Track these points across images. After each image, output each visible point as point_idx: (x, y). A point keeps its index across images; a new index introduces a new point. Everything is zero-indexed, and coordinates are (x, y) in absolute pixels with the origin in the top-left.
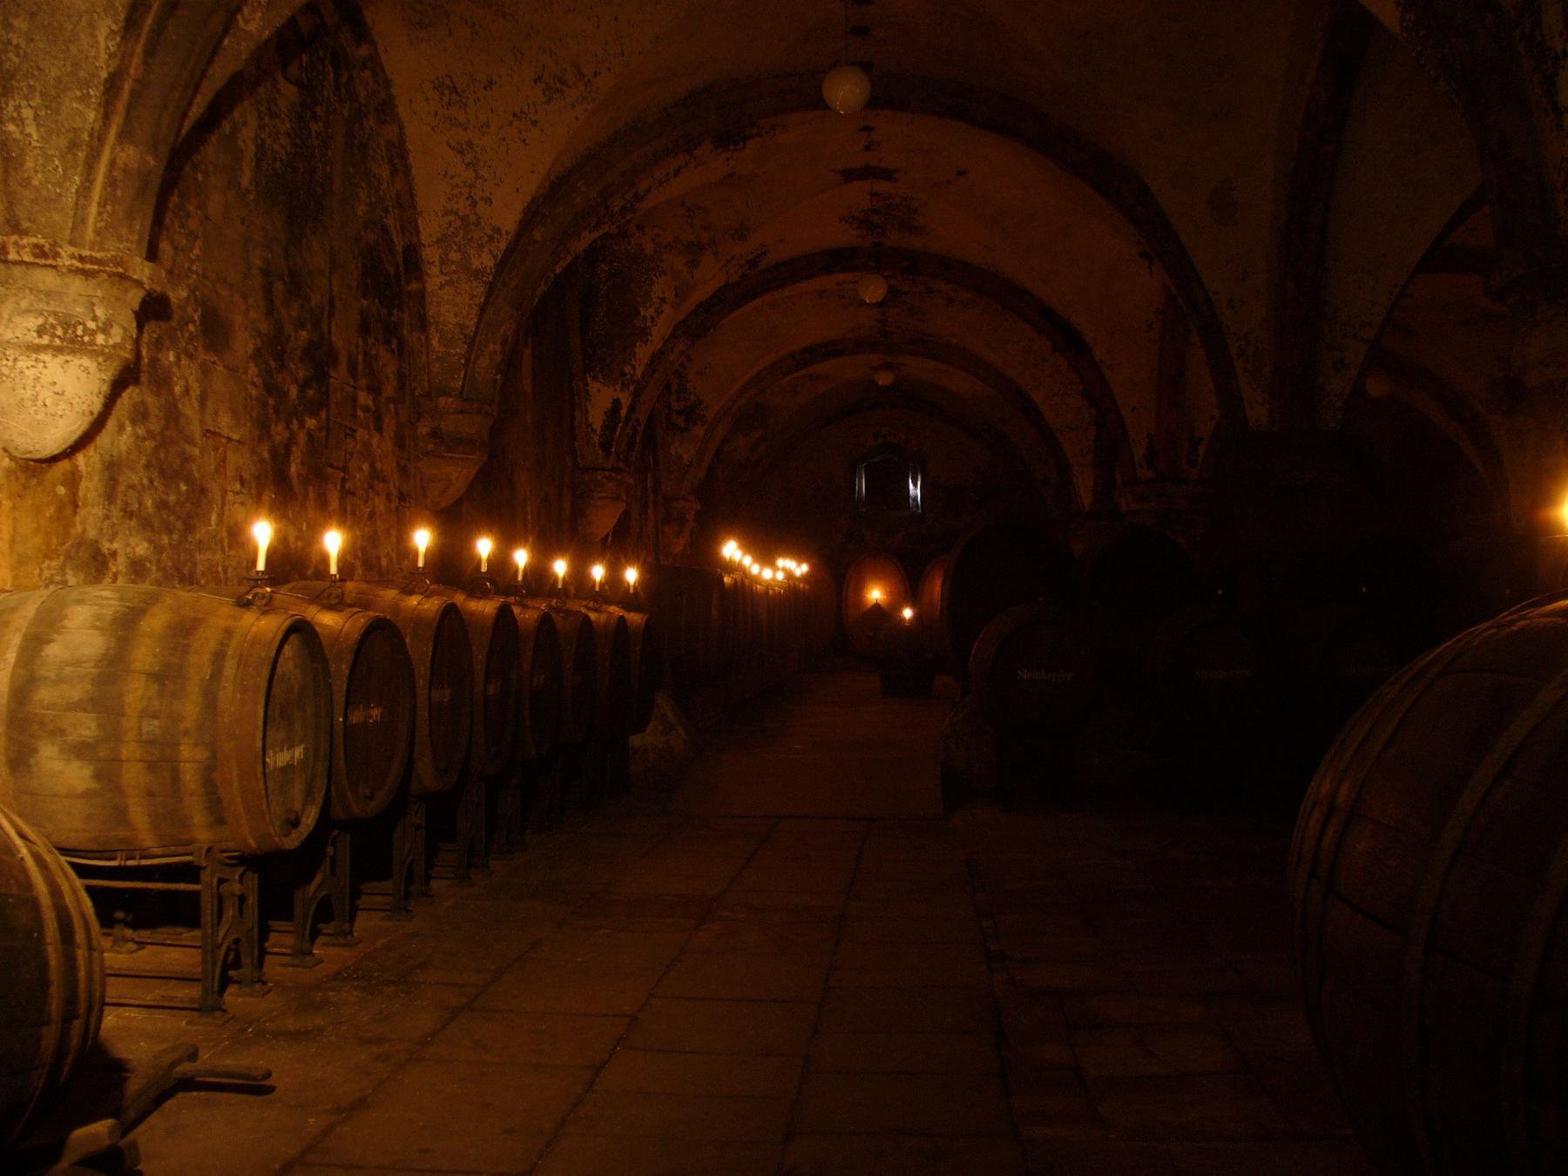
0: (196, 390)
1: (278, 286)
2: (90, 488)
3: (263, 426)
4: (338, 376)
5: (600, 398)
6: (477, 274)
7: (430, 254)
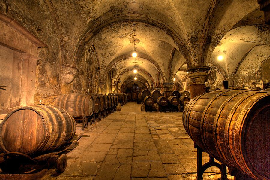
0: (81, 78)
1: (88, 70)
2: (72, 86)
3: (87, 81)
4: (93, 77)
5: (113, 80)
6: (104, 69)
7: (100, 68)
